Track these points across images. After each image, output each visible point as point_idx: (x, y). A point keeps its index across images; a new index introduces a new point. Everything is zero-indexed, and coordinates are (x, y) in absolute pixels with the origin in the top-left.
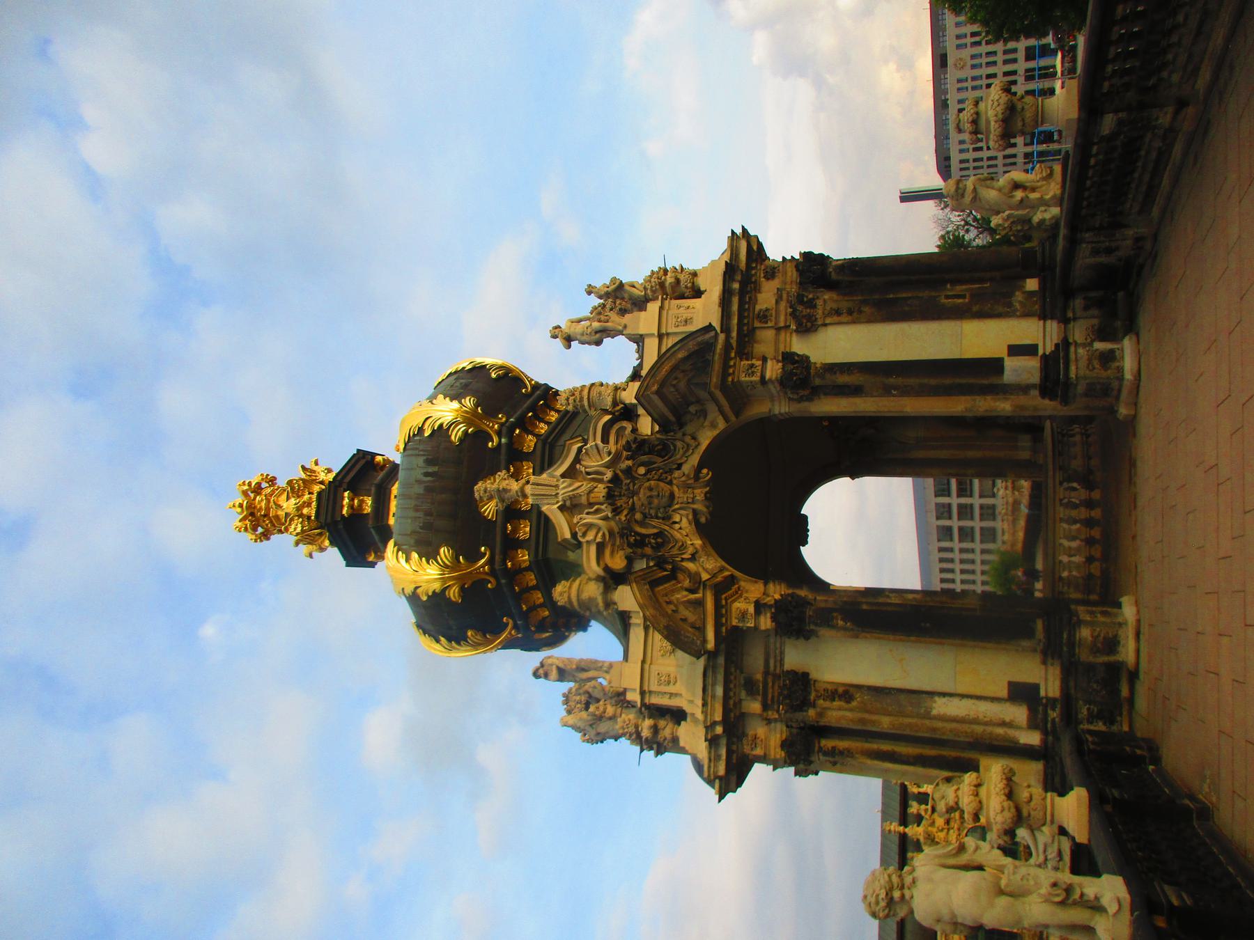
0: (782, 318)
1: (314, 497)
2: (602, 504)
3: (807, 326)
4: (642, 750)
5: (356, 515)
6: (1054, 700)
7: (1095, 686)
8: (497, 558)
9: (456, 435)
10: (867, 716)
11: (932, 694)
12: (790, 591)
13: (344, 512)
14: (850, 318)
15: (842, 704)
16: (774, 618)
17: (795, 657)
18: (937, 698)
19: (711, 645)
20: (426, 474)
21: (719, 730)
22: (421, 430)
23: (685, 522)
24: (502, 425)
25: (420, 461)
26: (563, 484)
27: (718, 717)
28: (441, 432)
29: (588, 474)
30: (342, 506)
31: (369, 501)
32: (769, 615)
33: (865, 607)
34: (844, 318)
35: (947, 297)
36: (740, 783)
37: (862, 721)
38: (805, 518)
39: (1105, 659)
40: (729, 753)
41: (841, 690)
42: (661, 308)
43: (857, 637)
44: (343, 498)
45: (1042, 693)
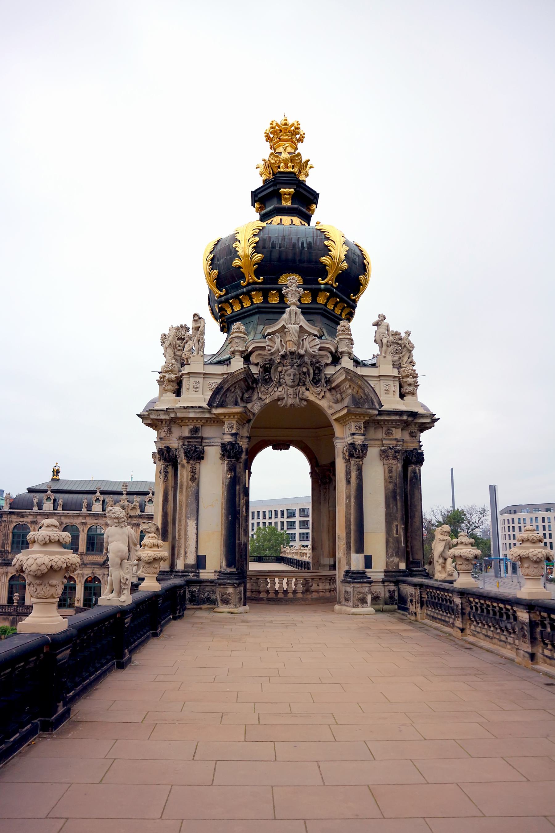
0: (388, 442)
1: (290, 170)
2: (286, 349)
3: (384, 454)
4: (159, 373)
5: (279, 196)
6: (199, 576)
7: (206, 594)
9: (324, 259)
10: (185, 488)
12: (244, 450)
13: (282, 190)
14: (387, 478)
15: (190, 477)
16: (230, 443)
17: (213, 453)
19: (214, 411)
21: (172, 415)
22: (328, 239)
23: (278, 393)
24: (332, 285)
25: (310, 240)
26: (297, 327)
27: (179, 415)
28: (326, 250)
29: (303, 340)
31: (289, 204)
32: (231, 440)
33: (237, 487)
34: (387, 475)
35: (397, 526)
36: (148, 425)
37: (181, 486)
38: (287, 448)
39: (219, 599)
40: (161, 420)
41: (196, 476)
42: (394, 377)
43: (223, 484)
44: (289, 188)
45: (201, 571)
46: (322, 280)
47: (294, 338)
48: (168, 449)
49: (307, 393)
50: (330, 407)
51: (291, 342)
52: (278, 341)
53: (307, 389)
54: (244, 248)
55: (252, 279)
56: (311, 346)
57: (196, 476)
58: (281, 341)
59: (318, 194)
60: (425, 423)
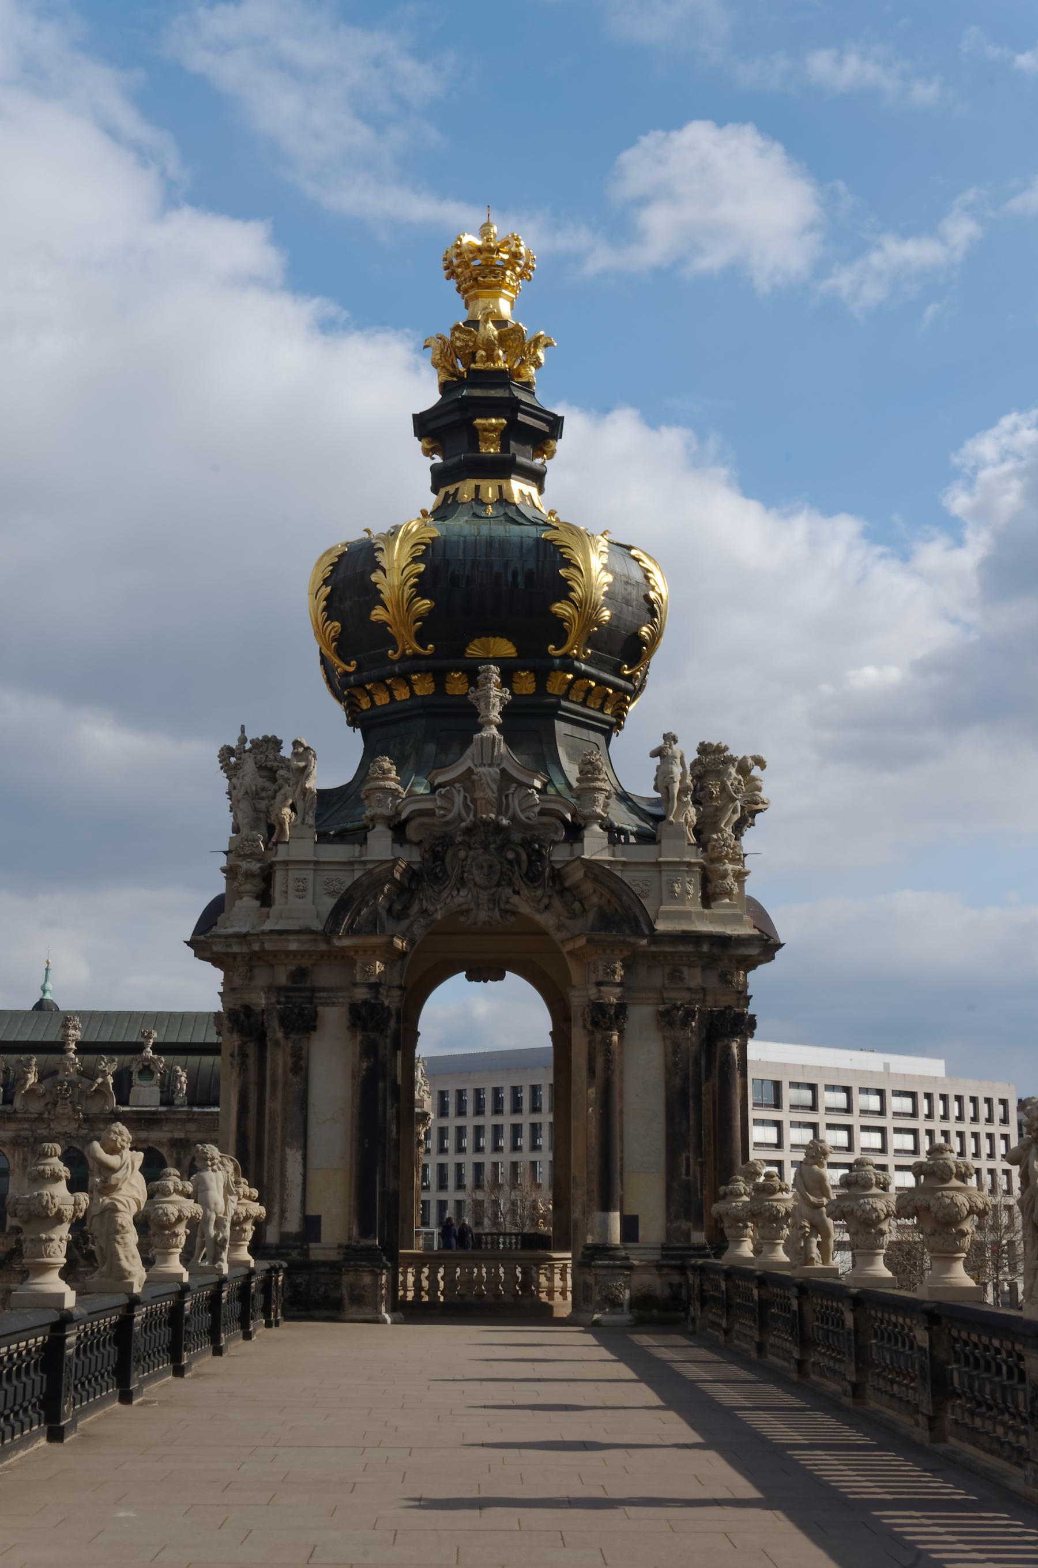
0: (672, 995)
2: (475, 816)
3: (668, 1019)
4: (226, 853)
6: (307, 1256)
7: (322, 1289)
8: (423, 662)
9: (561, 608)
10: (280, 1087)
11: (305, 1147)
12: (393, 1012)
15: (290, 1065)
16: (365, 1002)
17: (333, 1018)
18: (301, 1152)
19: (337, 943)
20: (515, 574)
21: (256, 947)
23: (460, 900)
25: (531, 565)
26: (494, 771)
29: (507, 796)
30: (487, 417)
32: (368, 996)
33: (381, 1085)
35: (688, 1159)
37: (274, 1083)
38: (500, 977)
39: (346, 1297)
40: (234, 956)
41: (302, 1063)
43: (353, 1077)
44: (496, 417)
45: (312, 1245)
46: (556, 649)
47: (490, 793)
48: (247, 1009)
49: (515, 899)
50: (560, 927)
51: (484, 802)
52: (459, 800)
53: (517, 893)
54: (396, 571)
55: (410, 648)
56: (524, 807)
57: (302, 1063)
58: (465, 797)
59: (562, 418)
60: (750, 956)
